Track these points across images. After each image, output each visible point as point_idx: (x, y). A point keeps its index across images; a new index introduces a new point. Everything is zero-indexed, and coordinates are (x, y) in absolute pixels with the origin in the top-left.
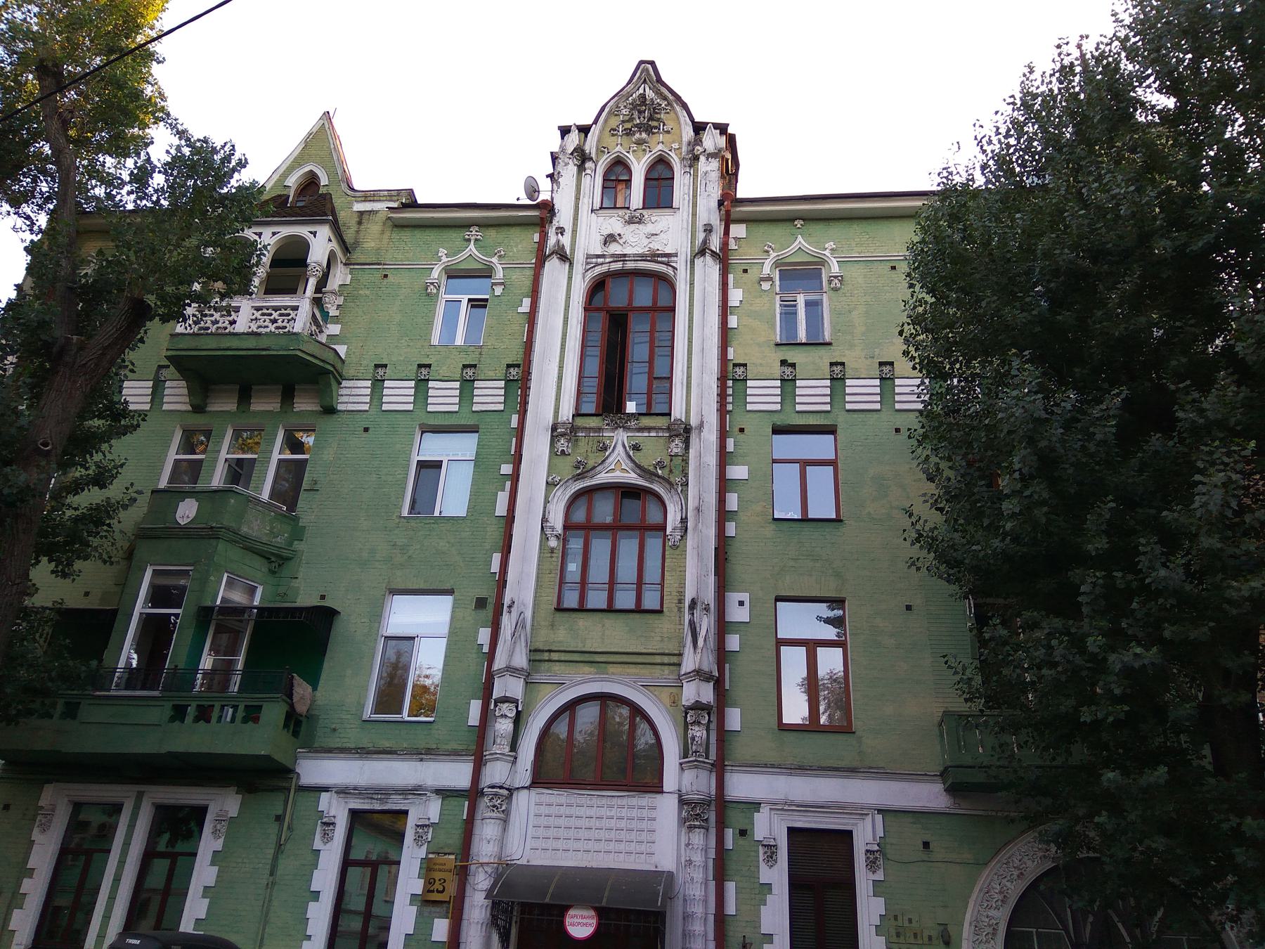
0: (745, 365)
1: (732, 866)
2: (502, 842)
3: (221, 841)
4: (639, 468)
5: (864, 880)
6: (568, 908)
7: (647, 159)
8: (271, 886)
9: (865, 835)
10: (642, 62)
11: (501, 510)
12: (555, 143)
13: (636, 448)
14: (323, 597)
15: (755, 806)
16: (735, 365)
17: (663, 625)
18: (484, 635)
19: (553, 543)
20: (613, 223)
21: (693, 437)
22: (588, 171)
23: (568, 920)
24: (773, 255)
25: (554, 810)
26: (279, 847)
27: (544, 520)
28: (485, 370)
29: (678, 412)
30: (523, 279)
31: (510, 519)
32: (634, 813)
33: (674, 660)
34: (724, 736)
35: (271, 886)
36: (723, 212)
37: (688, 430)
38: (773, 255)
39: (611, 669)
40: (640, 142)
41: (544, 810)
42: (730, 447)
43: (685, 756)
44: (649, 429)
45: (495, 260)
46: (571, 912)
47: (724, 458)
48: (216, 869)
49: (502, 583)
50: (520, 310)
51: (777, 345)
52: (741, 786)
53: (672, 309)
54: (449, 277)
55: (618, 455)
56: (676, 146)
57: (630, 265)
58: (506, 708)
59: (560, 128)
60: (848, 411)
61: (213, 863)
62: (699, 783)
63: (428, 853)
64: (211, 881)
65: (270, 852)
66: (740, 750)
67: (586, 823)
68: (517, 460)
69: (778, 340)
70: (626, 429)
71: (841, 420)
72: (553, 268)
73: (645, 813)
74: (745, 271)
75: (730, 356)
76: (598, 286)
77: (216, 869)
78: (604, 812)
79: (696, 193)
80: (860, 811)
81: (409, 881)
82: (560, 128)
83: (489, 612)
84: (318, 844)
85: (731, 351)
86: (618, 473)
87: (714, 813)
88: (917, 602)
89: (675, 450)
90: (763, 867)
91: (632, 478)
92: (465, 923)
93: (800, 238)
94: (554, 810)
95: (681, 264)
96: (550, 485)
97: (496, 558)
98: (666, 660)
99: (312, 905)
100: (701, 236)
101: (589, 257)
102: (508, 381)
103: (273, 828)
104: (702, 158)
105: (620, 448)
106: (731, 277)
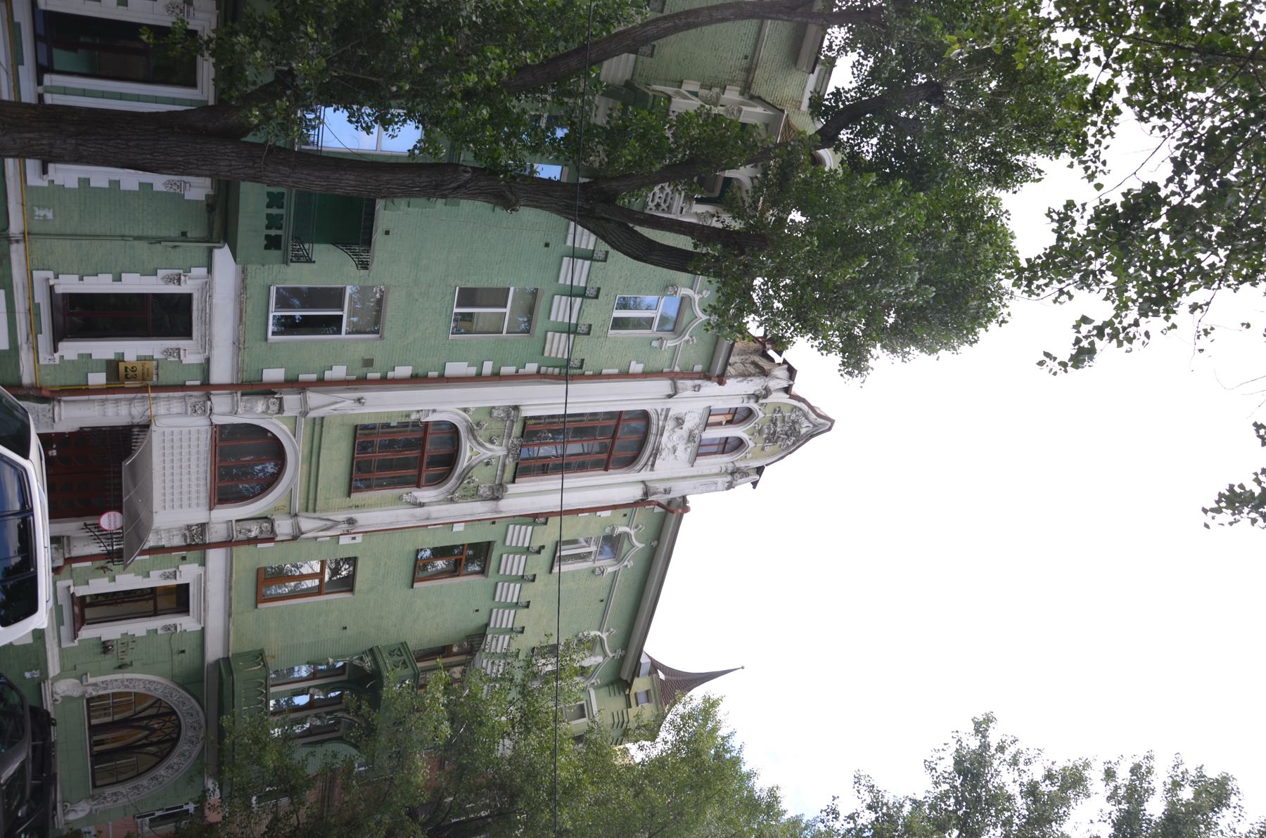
0: (546, 523)
1: (160, 556)
2: (169, 415)
3: (163, 189)
4: (470, 468)
5: (158, 623)
6: (121, 512)
7: (745, 437)
8: (123, 237)
9: (187, 623)
10: (832, 422)
11: (453, 369)
13: (487, 464)
14: (387, 233)
15: (203, 563)
17: (341, 500)
18: (339, 372)
19: (414, 417)
21: (491, 504)
23: (112, 513)
25: (194, 443)
26: (159, 240)
27: (434, 411)
28: (582, 340)
29: (512, 488)
30: (661, 362)
31: (443, 380)
32: (194, 495)
33: (311, 506)
34: (256, 540)
35: (123, 237)
37: (497, 499)
38: (632, 532)
39: (306, 467)
40: (760, 432)
41: (194, 437)
43: (237, 521)
44: (503, 471)
46: (118, 514)
48: (137, 188)
49: (385, 382)
50: (633, 363)
52: (216, 558)
54: (682, 299)
55: (485, 454)
56: (749, 456)
57: (652, 439)
58: (275, 408)
60: (491, 611)
61: (141, 184)
62: (217, 533)
63: (157, 360)
64: (125, 186)
65: (153, 232)
66: (241, 551)
67: (185, 464)
68: (496, 377)
70: (507, 456)
71: (491, 579)
72: (664, 386)
73: (194, 502)
76: (645, 416)
77: (137, 188)
78: (194, 477)
80: (202, 618)
81: (133, 350)
83: (359, 372)
84: (161, 273)
86: (468, 454)
87: (196, 543)
88: (348, 631)
90: (161, 572)
91: (463, 463)
92: (103, 397)
93: (641, 546)
94: (194, 443)
95: (645, 475)
96: (465, 410)
97: (404, 371)
98: (311, 502)
99: (110, 276)
100: (661, 487)
101: (668, 410)
103: (174, 232)
104: (729, 478)
105: (490, 454)
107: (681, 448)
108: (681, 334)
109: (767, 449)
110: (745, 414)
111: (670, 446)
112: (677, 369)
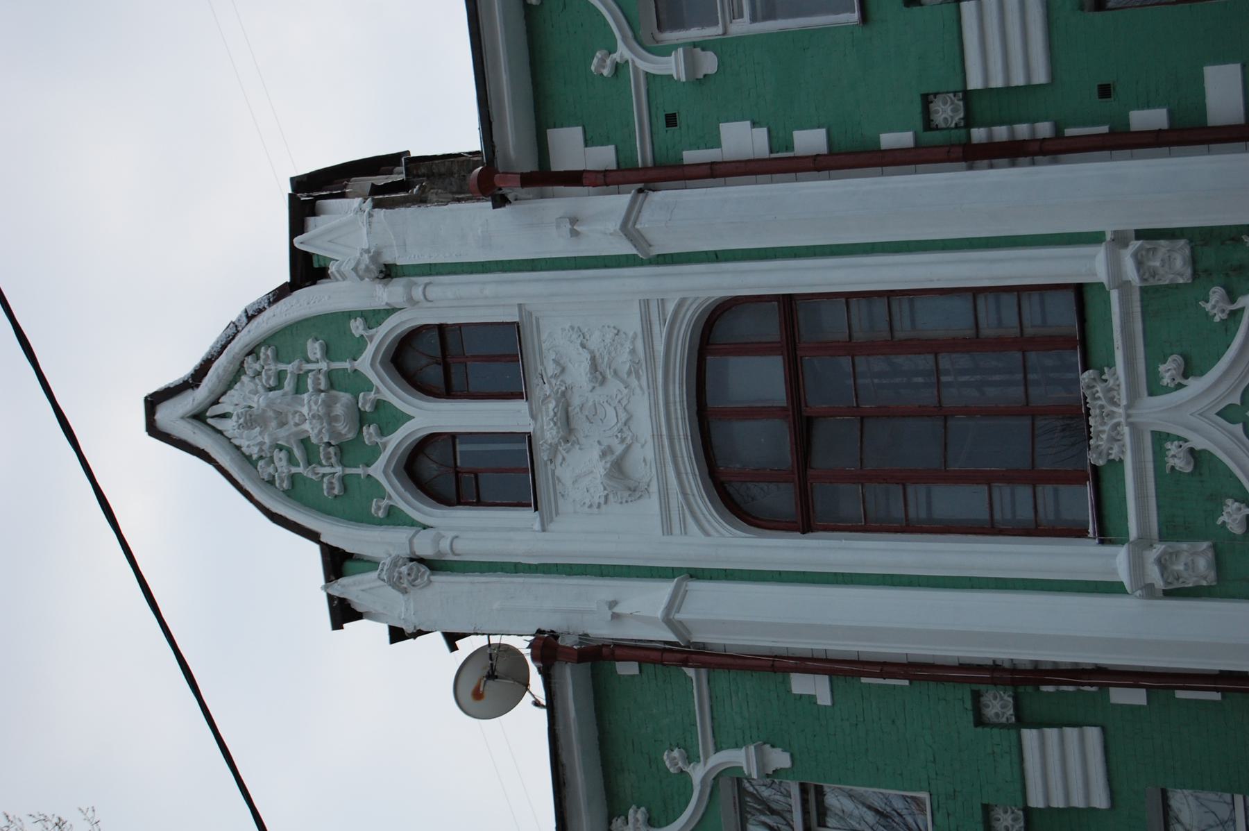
0: (926, 100)
10: (153, 430)
12: (367, 634)
16: (928, 124)
20: (576, 472)
22: (445, 545)
24: (623, 52)
36: (522, 192)
38: (623, 52)
42: (1150, 118)
45: (697, 773)
47: (1191, 132)
50: (824, 699)
51: (865, 18)
53: (788, 304)
56: (357, 327)
59: (337, 624)
69: (855, 17)
74: (671, 120)
75: (904, 139)
79: (465, 261)
82: (337, 624)
85: (889, 140)
89: (1179, 262)
101: (667, 529)
102: (1022, 720)
106: (691, 156)
107: (579, 373)
108: (716, 781)
109: (314, 349)
110: (429, 468)
111: (614, 386)
112: (690, 672)
